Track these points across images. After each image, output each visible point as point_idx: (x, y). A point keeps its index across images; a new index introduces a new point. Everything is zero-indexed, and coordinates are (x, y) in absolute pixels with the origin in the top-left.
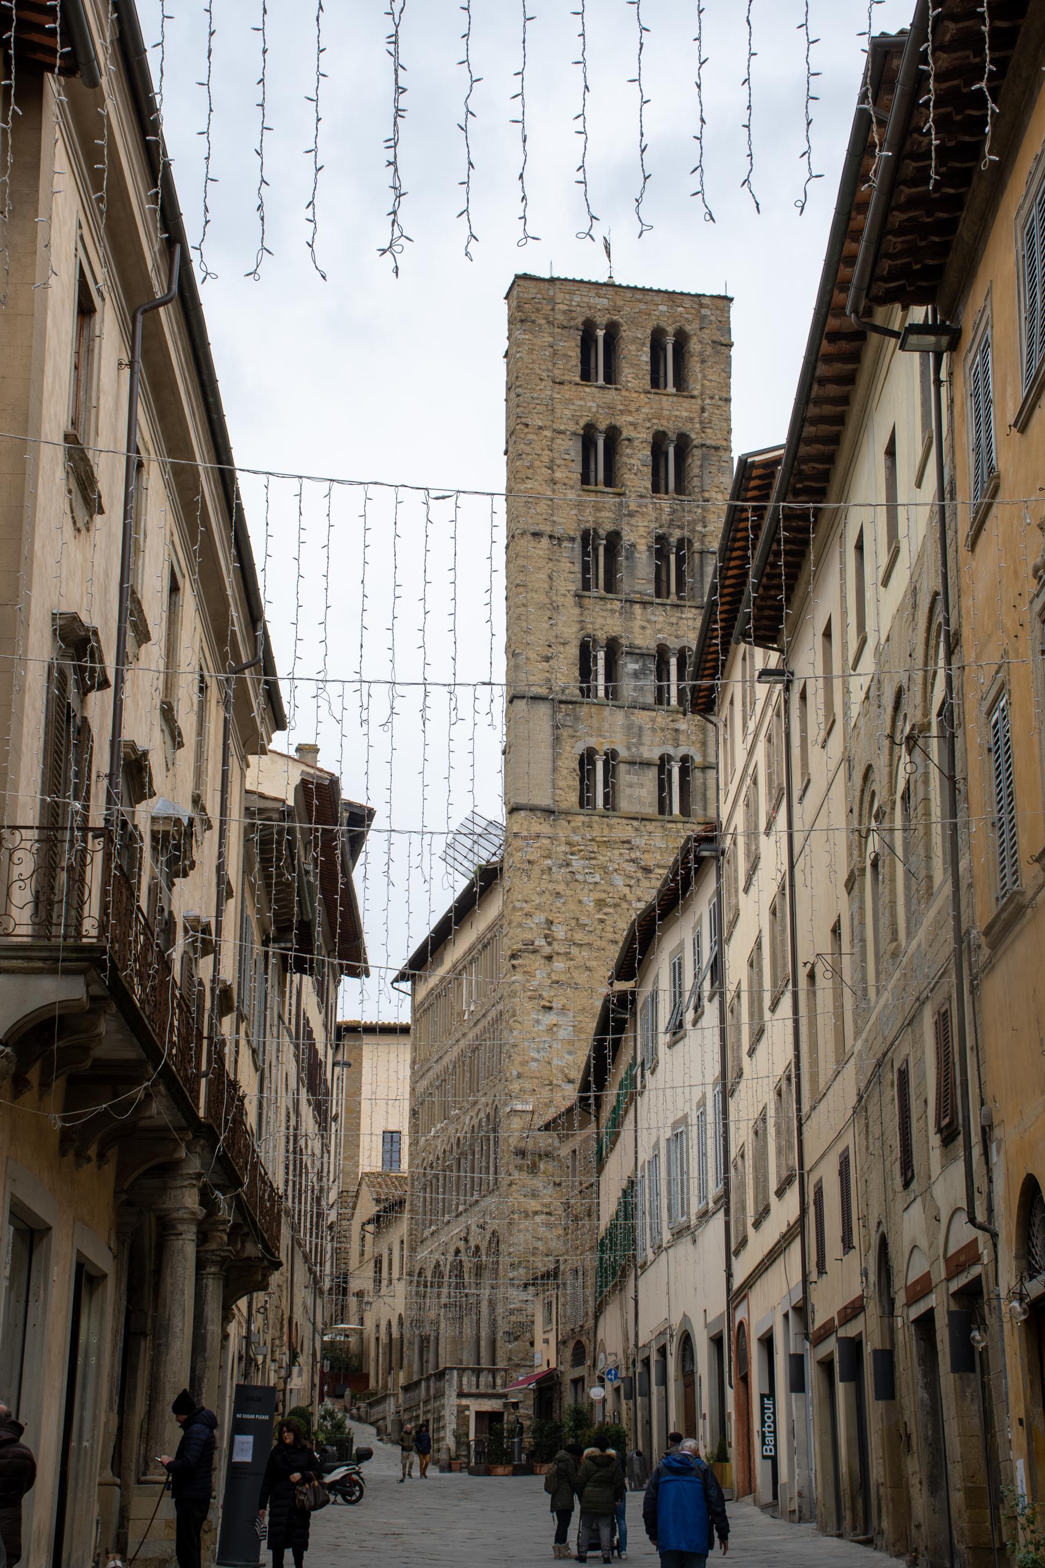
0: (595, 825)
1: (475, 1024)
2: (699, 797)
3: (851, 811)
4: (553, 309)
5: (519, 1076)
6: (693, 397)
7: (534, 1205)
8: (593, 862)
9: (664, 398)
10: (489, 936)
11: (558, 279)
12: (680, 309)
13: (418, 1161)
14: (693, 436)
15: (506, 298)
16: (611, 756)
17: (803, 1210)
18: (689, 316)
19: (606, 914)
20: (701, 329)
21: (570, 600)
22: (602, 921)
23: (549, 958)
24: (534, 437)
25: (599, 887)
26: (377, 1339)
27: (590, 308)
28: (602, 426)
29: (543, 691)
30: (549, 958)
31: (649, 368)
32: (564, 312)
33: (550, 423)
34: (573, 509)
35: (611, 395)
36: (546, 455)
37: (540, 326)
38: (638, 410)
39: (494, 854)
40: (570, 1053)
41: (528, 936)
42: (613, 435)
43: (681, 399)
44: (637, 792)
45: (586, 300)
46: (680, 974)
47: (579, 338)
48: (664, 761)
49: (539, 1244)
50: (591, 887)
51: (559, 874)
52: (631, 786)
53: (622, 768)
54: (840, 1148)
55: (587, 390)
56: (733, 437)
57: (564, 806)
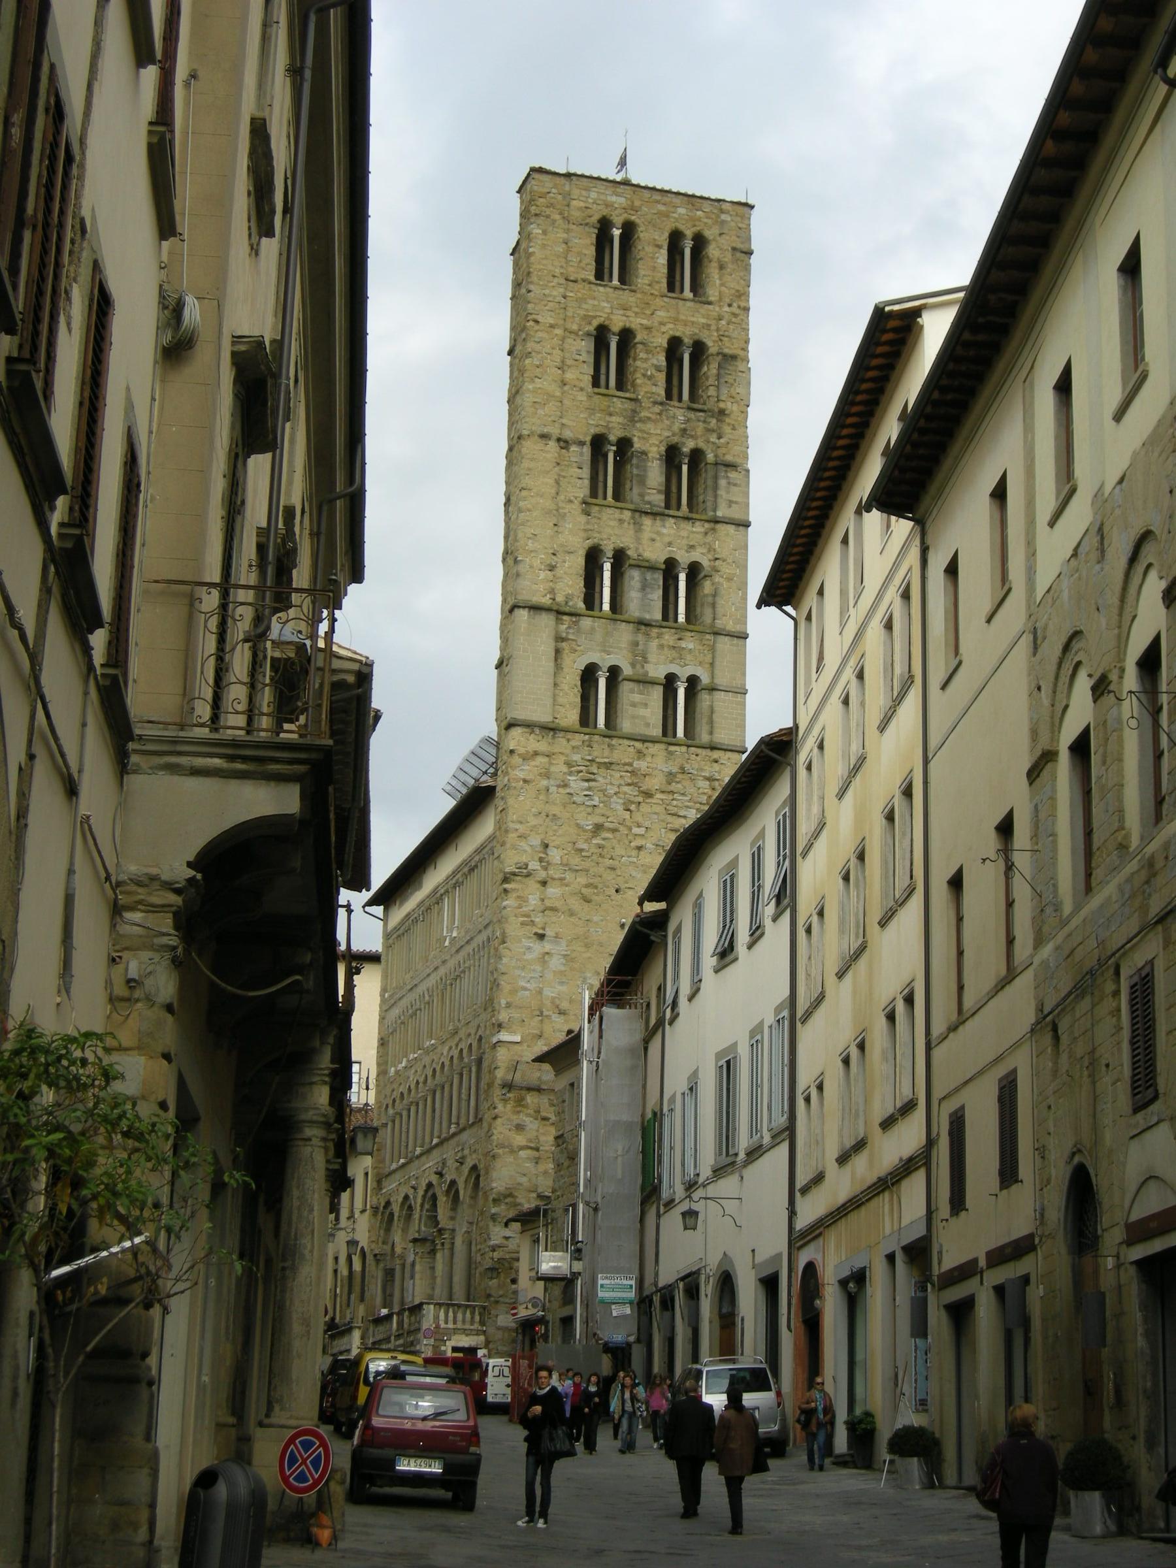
0: (595, 746)
1: (458, 951)
2: (705, 720)
3: (1039, 688)
4: (568, 206)
5: (508, 1005)
6: (710, 303)
8: (592, 784)
9: (681, 302)
10: (477, 858)
11: (575, 175)
12: (699, 213)
13: (388, 1091)
14: (710, 343)
15: (518, 192)
16: (614, 673)
17: (930, 1143)
18: (709, 221)
19: (604, 839)
20: (721, 234)
21: (576, 507)
22: (600, 847)
23: (544, 883)
24: (545, 335)
25: (597, 811)
26: (336, 1271)
27: (607, 206)
28: (616, 326)
29: (546, 601)
30: (544, 883)
31: (666, 271)
32: (580, 209)
33: (562, 322)
34: (585, 414)
35: (626, 297)
36: (557, 355)
37: (554, 221)
38: (654, 314)
39: (485, 773)
40: (562, 983)
41: (524, 859)
42: (626, 336)
43: (698, 305)
44: (642, 712)
45: (602, 197)
46: (732, 892)
47: (594, 236)
48: (671, 679)
49: (524, 1180)
50: (590, 810)
51: (557, 794)
52: (634, 705)
53: (625, 688)
54: (1001, 1071)
55: (601, 289)
56: (751, 348)
57: (563, 723)
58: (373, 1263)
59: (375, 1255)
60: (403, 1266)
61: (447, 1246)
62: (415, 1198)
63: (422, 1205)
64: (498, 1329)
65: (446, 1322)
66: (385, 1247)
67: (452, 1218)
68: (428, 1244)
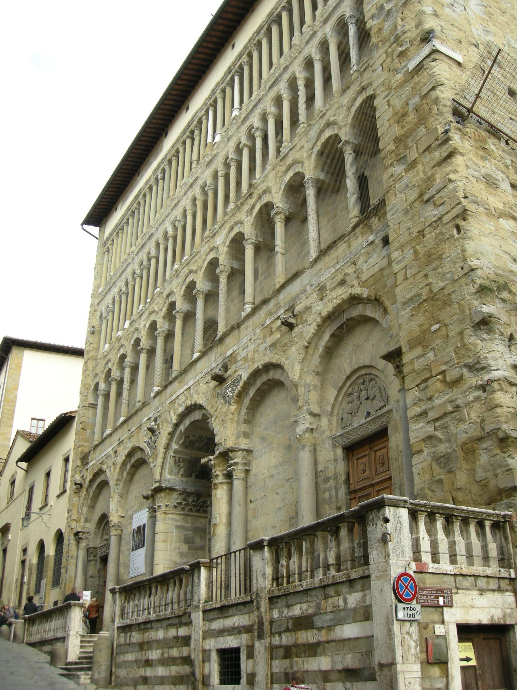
26: (23, 562)
58: (73, 542)
59: (77, 534)
60: (120, 537)
61: (238, 475)
63: (167, 447)
65: (435, 560)
66: (88, 525)
67: (246, 435)
68: (175, 495)
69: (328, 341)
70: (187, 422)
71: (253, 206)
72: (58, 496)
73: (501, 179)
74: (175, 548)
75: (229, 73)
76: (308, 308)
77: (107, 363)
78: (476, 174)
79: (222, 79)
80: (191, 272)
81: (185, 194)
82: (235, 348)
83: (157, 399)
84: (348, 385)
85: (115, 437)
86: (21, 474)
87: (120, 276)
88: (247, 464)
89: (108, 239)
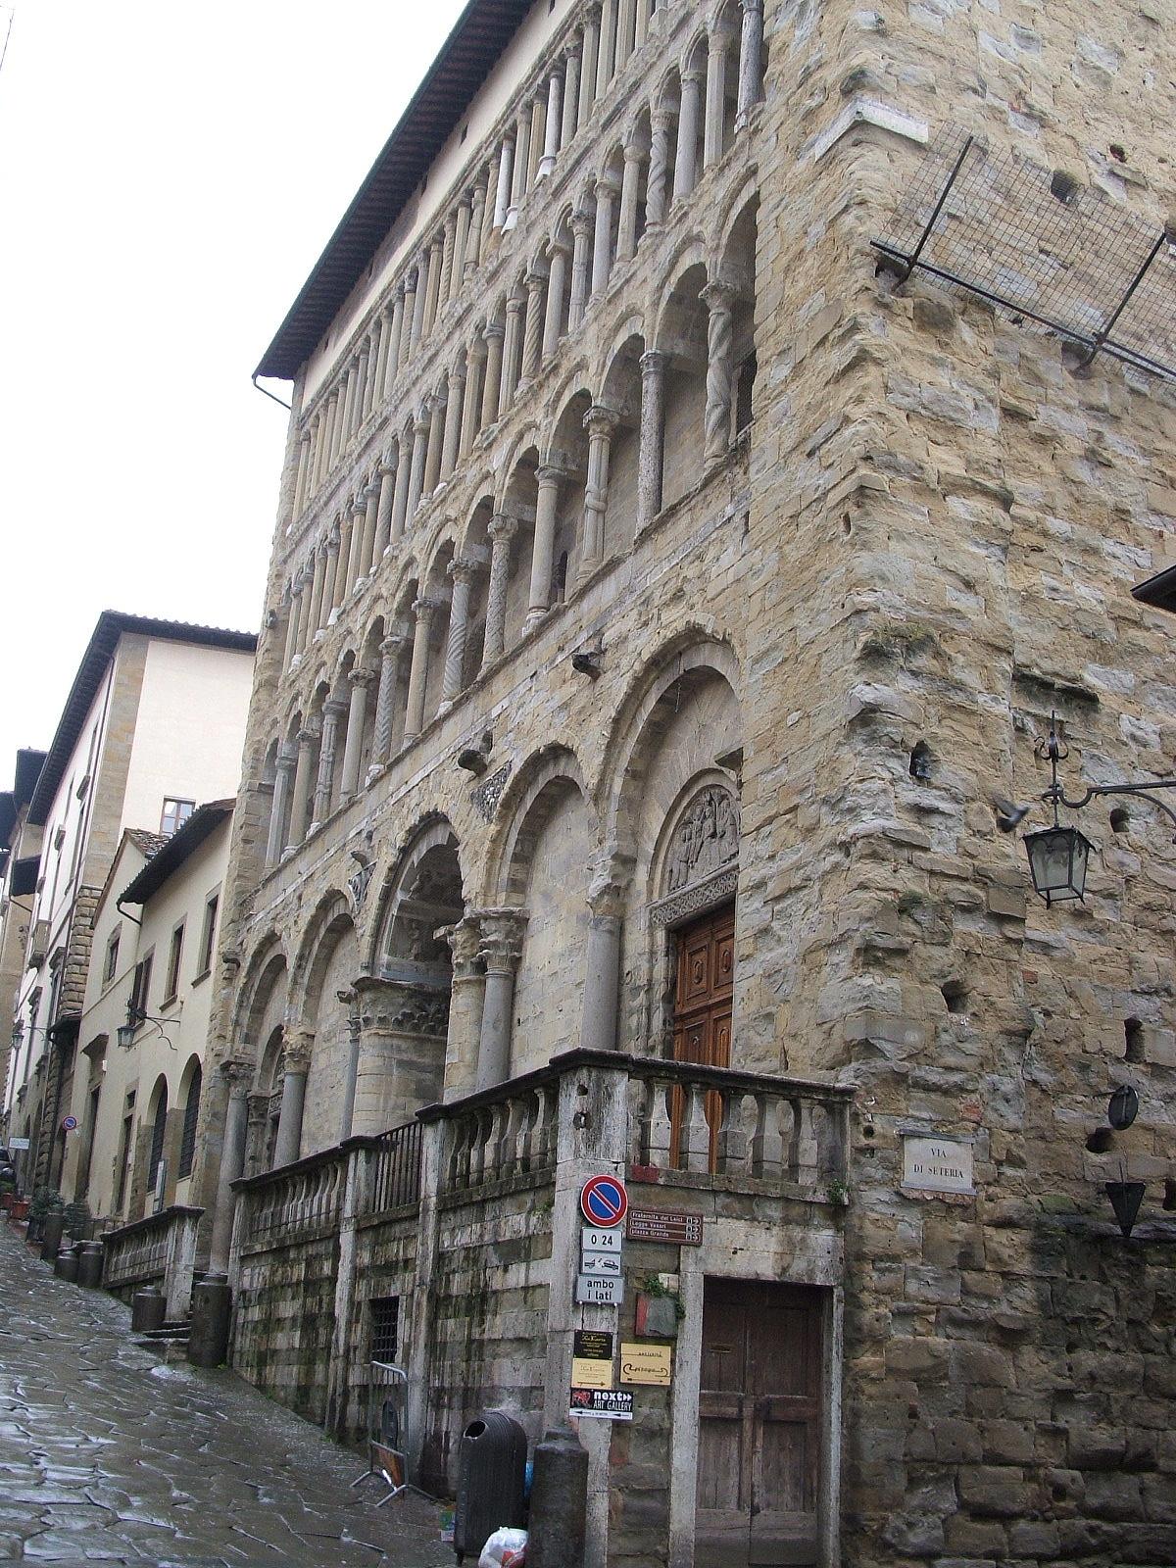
7: (945, 461)
26: (128, 1121)
49: (966, 602)
62: (361, 891)
63: (387, 896)
64: (904, 1200)
69: (653, 712)
70: (423, 848)
71: (559, 395)
72: (195, 984)
73: (970, 406)
74: (396, 1107)
75: (541, 69)
76: (623, 640)
77: (295, 699)
78: (905, 401)
79: (528, 80)
80: (448, 520)
81: (448, 338)
82: (505, 703)
83: (373, 793)
84: (684, 804)
85: (302, 865)
86: (129, 930)
87: (326, 504)
88: (518, 946)
89: (309, 411)
